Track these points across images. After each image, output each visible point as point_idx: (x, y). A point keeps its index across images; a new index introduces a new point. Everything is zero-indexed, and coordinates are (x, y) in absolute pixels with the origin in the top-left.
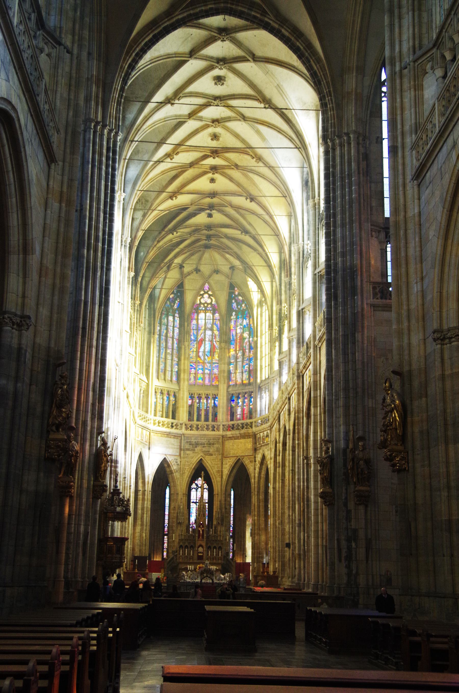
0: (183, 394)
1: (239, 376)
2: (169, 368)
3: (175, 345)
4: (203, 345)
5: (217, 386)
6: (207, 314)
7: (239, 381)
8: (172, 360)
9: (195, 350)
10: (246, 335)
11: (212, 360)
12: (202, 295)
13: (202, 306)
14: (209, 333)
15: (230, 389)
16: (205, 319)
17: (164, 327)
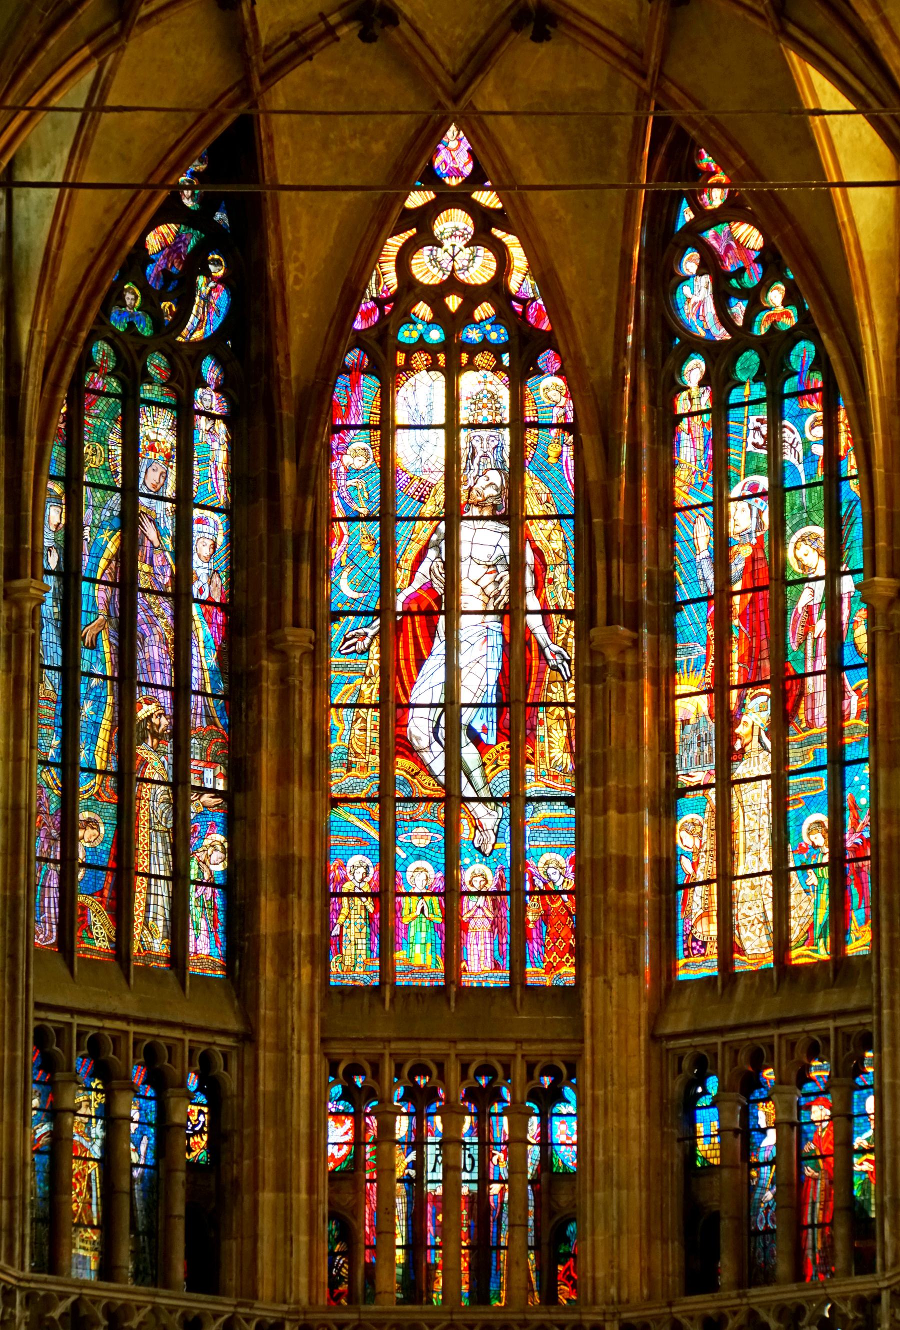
0: (284, 1072)
1: (753, 901)
2: (152, 855)
3: (204, 658)
4: (439, 647)
5: (568, 997)
6: (469, 382)
7: (755, 944)
8: (179, 785)
9: (370, 692)
10: (805, 553)
11: (517, 778)
12: (422, 219)
13: (423, 310)
14: (483, 542)
15: (679, 1021)
16: (452, 427)
17: (100, 509)
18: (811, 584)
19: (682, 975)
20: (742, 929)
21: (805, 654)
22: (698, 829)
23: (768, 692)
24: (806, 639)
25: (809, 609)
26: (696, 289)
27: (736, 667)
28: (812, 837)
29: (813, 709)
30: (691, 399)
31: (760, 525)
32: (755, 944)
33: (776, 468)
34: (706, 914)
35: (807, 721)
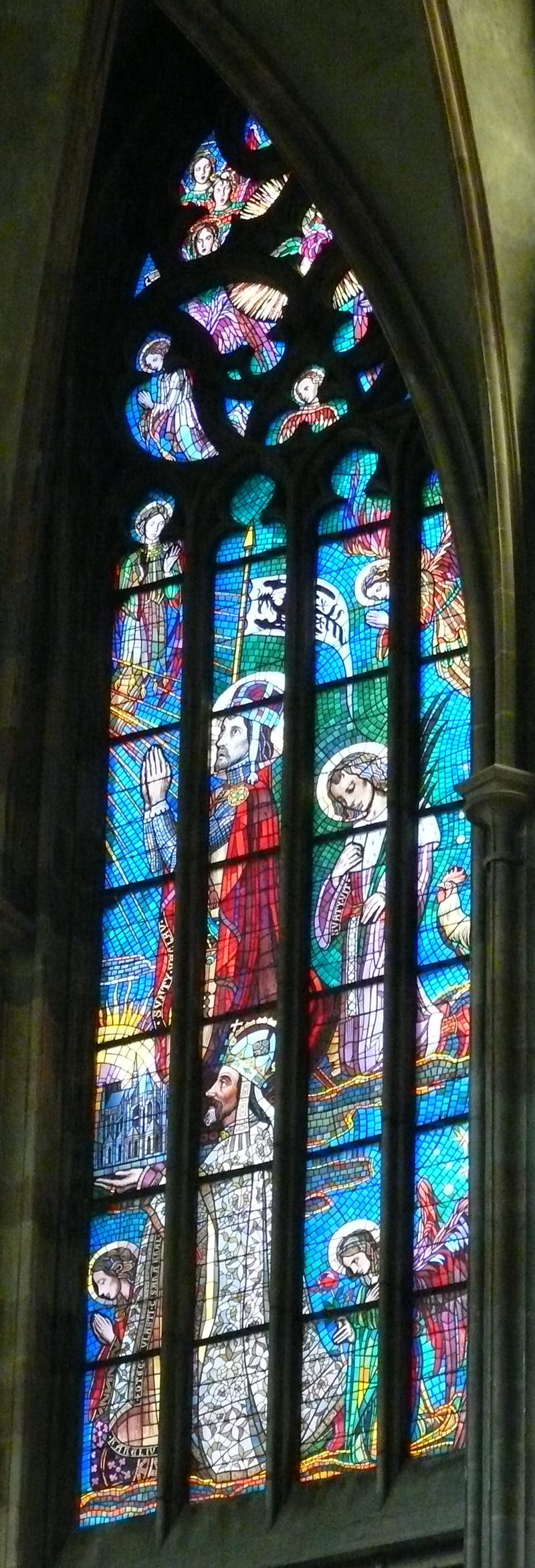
7: (231, 1452)
18: (359, 839)
19: (89, 1518)
20: (206, 1431)
21: (344, 952)
22: (129, 1266)
23: (273, 1023)
24: (345, 928)
25: (353, 880)
26: (163, 393)
27: (212, 987)
28: (347, 1261)
29: (356, 1043)
30: (145, 563)
31: (266, 749)
32: (231, 1452)
33: (300, 652)
34: (139, 1406)
35: (343, 1064)
